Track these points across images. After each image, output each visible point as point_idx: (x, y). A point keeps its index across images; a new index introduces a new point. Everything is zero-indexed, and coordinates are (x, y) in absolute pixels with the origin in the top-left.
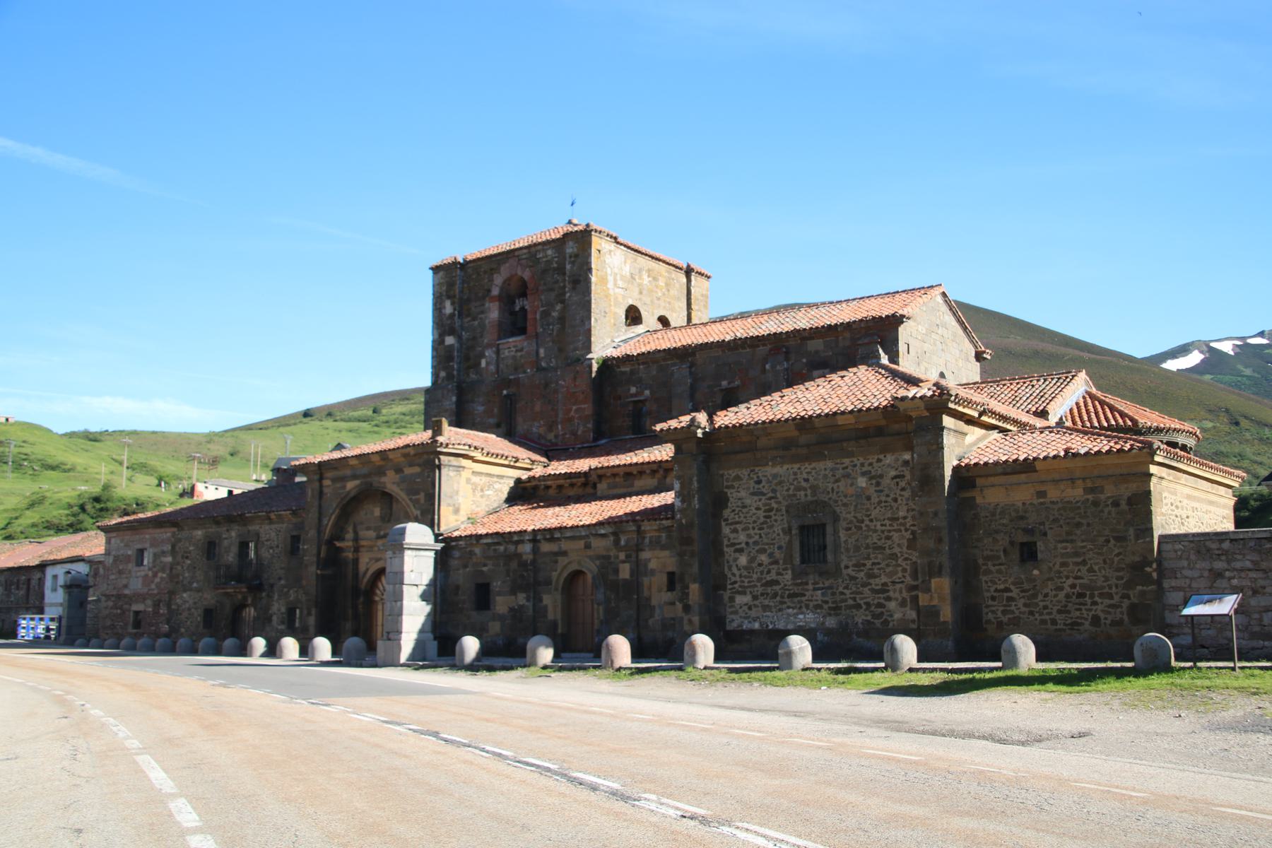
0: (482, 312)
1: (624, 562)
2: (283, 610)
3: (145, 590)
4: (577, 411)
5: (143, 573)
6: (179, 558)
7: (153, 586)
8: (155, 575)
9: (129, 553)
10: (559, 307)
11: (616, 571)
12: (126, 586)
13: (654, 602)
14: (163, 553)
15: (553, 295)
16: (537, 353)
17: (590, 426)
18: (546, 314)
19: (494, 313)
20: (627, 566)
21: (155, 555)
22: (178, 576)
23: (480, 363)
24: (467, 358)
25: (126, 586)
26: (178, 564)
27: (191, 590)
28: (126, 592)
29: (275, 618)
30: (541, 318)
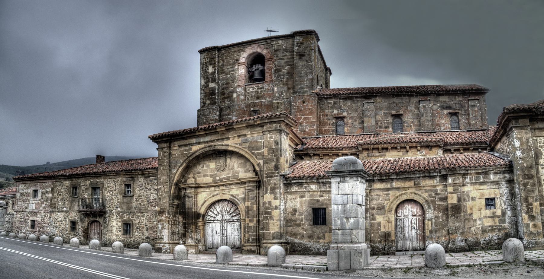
0: (233, 71)
1: (451, 193)
2: (120, 224)
3: (37, 210)
4: (305, 119)
5: (36, 202)
6: (56, 195)
7: (41, 208)
8: (42, 203)
9: (29, 191)
10: (287, 68)
11: (445, 199)
12: (26, 208)
13: (475, 217)
14: (47, 192)
15: (283, 62)
16: (273, 90)
17: (315, 127)
18: (278, 71)
19: (242, 71)
20: (455, 196)
21: (42, 193)
22: (55, 204)
23: (232, 96)
24: (223, 94)
25: (26, 208)
26: (55, 198)
27: (62, 212)
28: (27, 210)
29: (114, 229)
30: (275, 72)
